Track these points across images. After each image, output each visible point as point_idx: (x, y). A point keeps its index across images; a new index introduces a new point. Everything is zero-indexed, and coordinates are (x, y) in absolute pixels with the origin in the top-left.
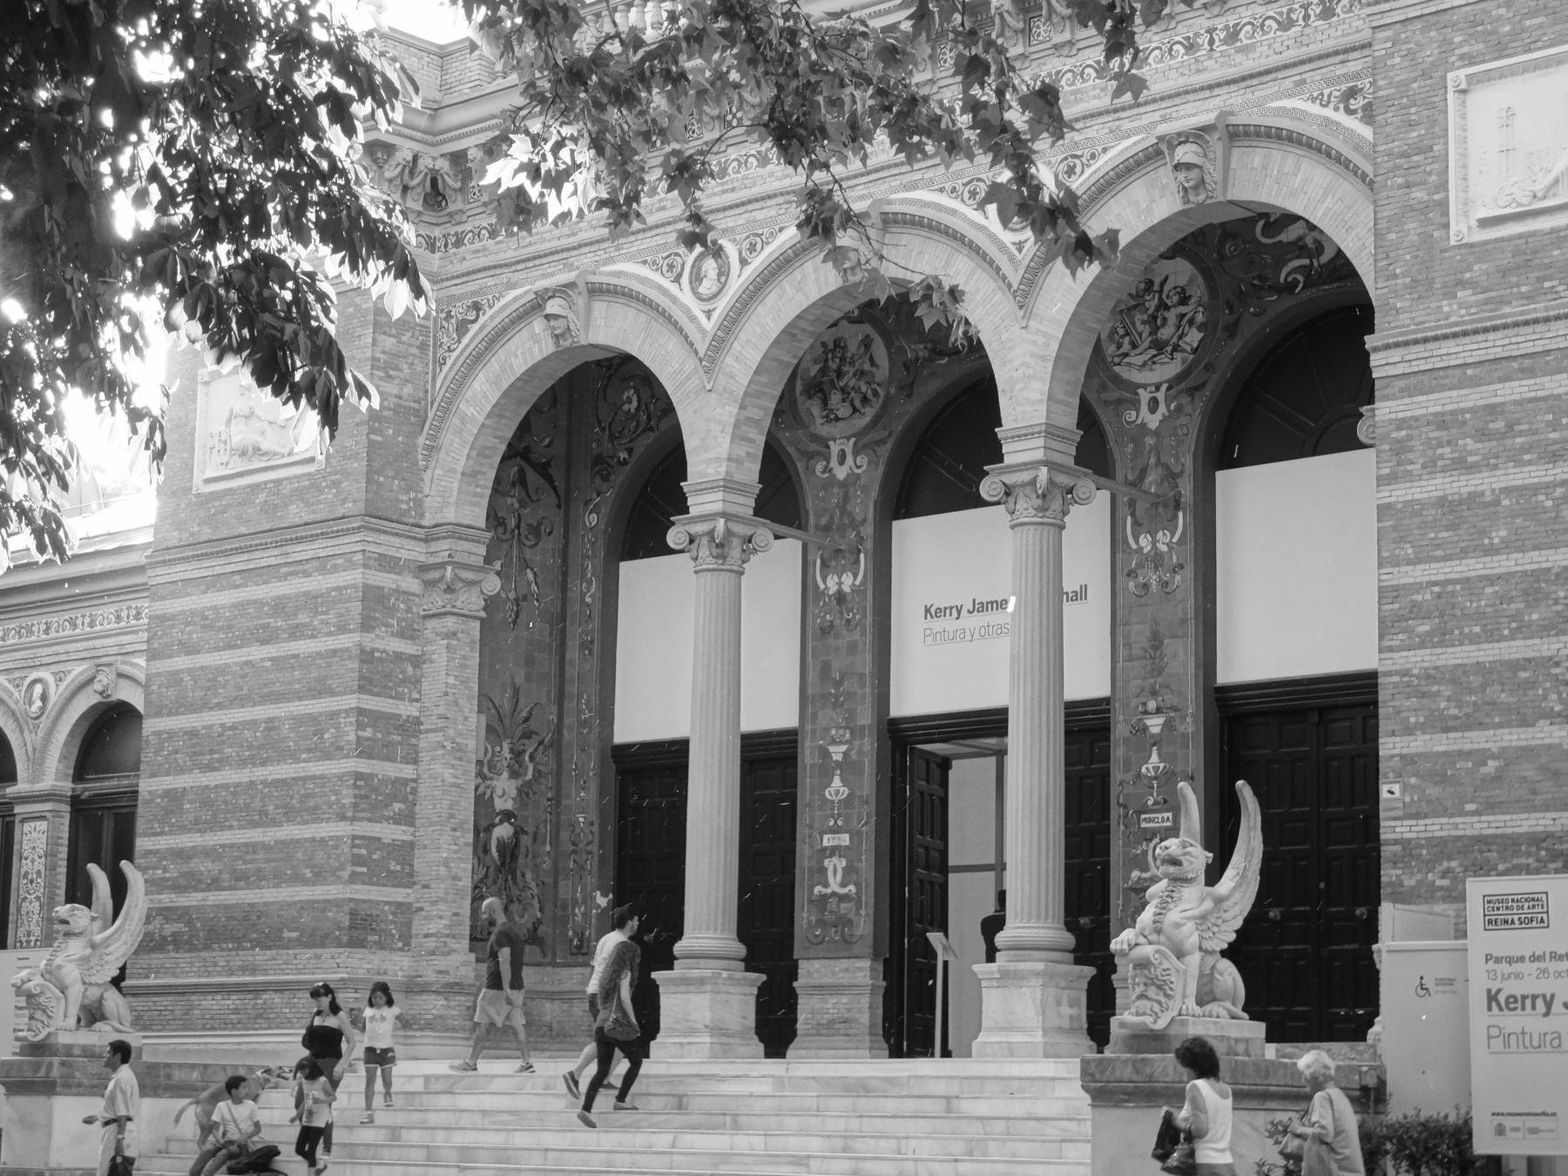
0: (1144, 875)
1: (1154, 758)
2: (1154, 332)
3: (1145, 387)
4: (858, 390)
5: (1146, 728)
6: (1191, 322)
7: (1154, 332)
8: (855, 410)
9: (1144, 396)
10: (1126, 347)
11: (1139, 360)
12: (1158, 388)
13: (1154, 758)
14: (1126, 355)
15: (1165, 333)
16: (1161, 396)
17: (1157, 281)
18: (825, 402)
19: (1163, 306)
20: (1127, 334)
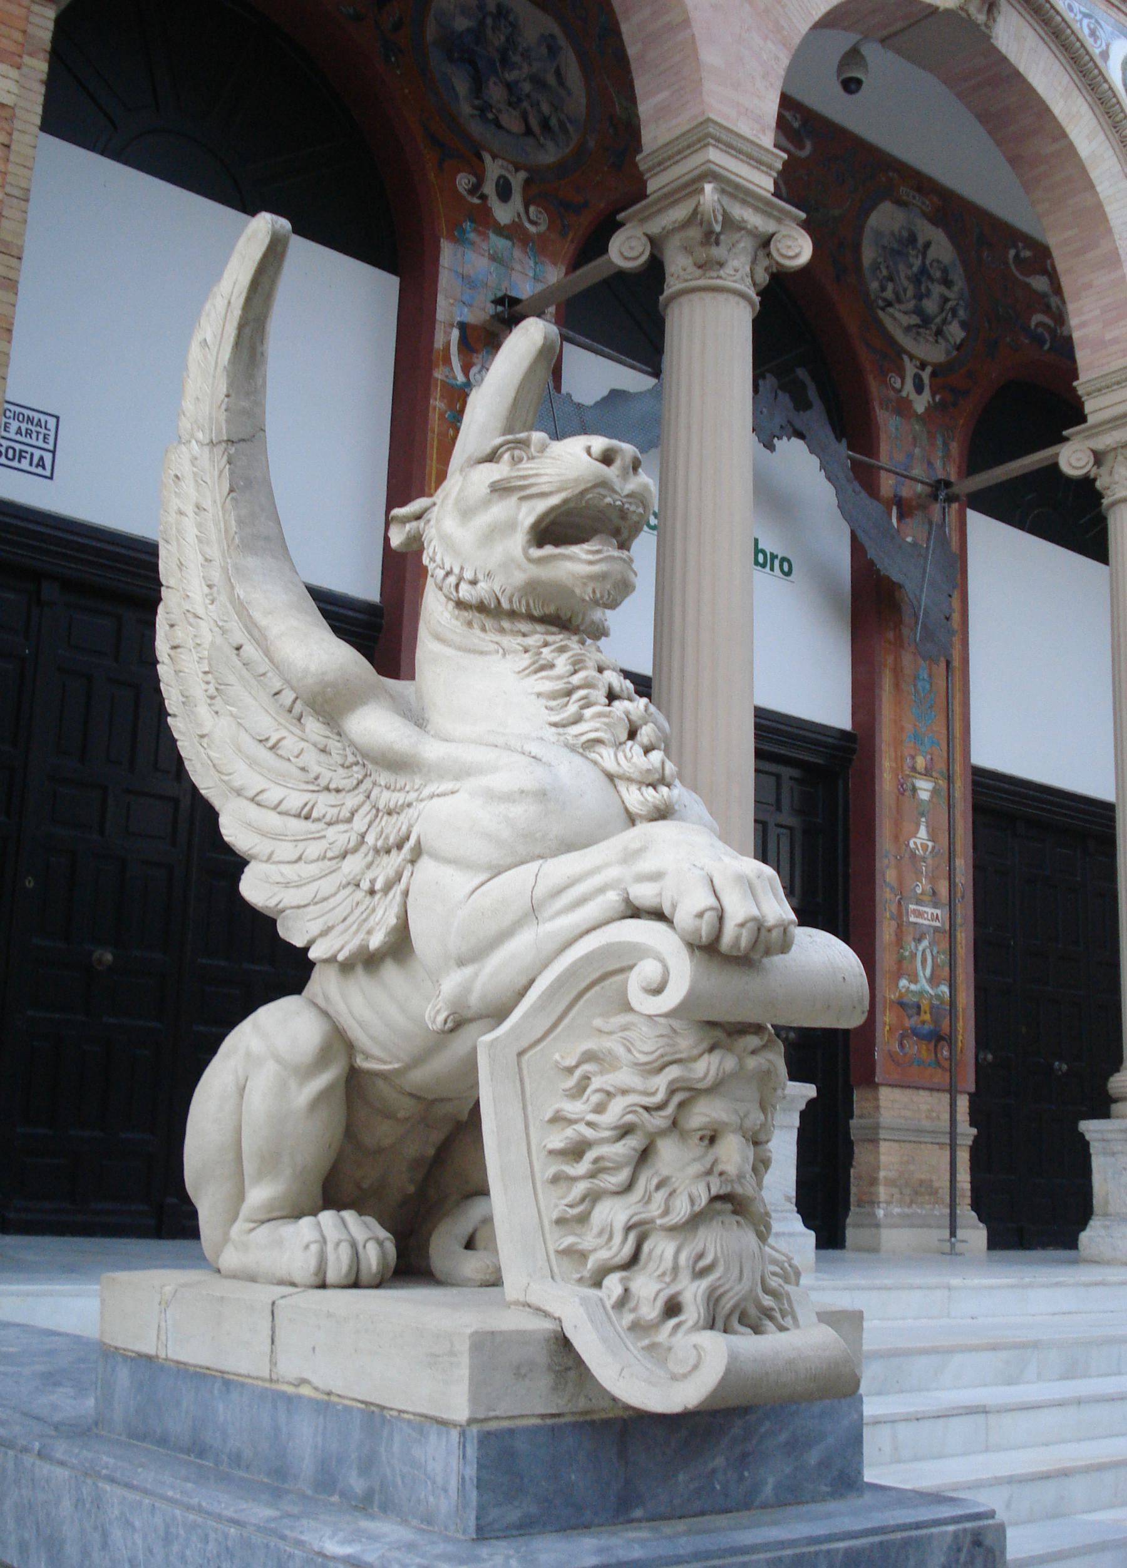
0: (913, 987)
1: (923, 832)
2: (919, 297)
3: (912, 357)
4: (536, 105)
5: (914, 789)
6: (954, 311)
7: (919, 297)
8: (529, 132)
9: (910, 369)
10: (889, 294)
11: (905, 320)
12: (923, 366)
13: (923, 832)
14: (889, 304)
15: (930, 306)
16: (926, 375)
17: (921, 242)
18: (478, 87)
19: (923, 271)
20: (891, 279)
